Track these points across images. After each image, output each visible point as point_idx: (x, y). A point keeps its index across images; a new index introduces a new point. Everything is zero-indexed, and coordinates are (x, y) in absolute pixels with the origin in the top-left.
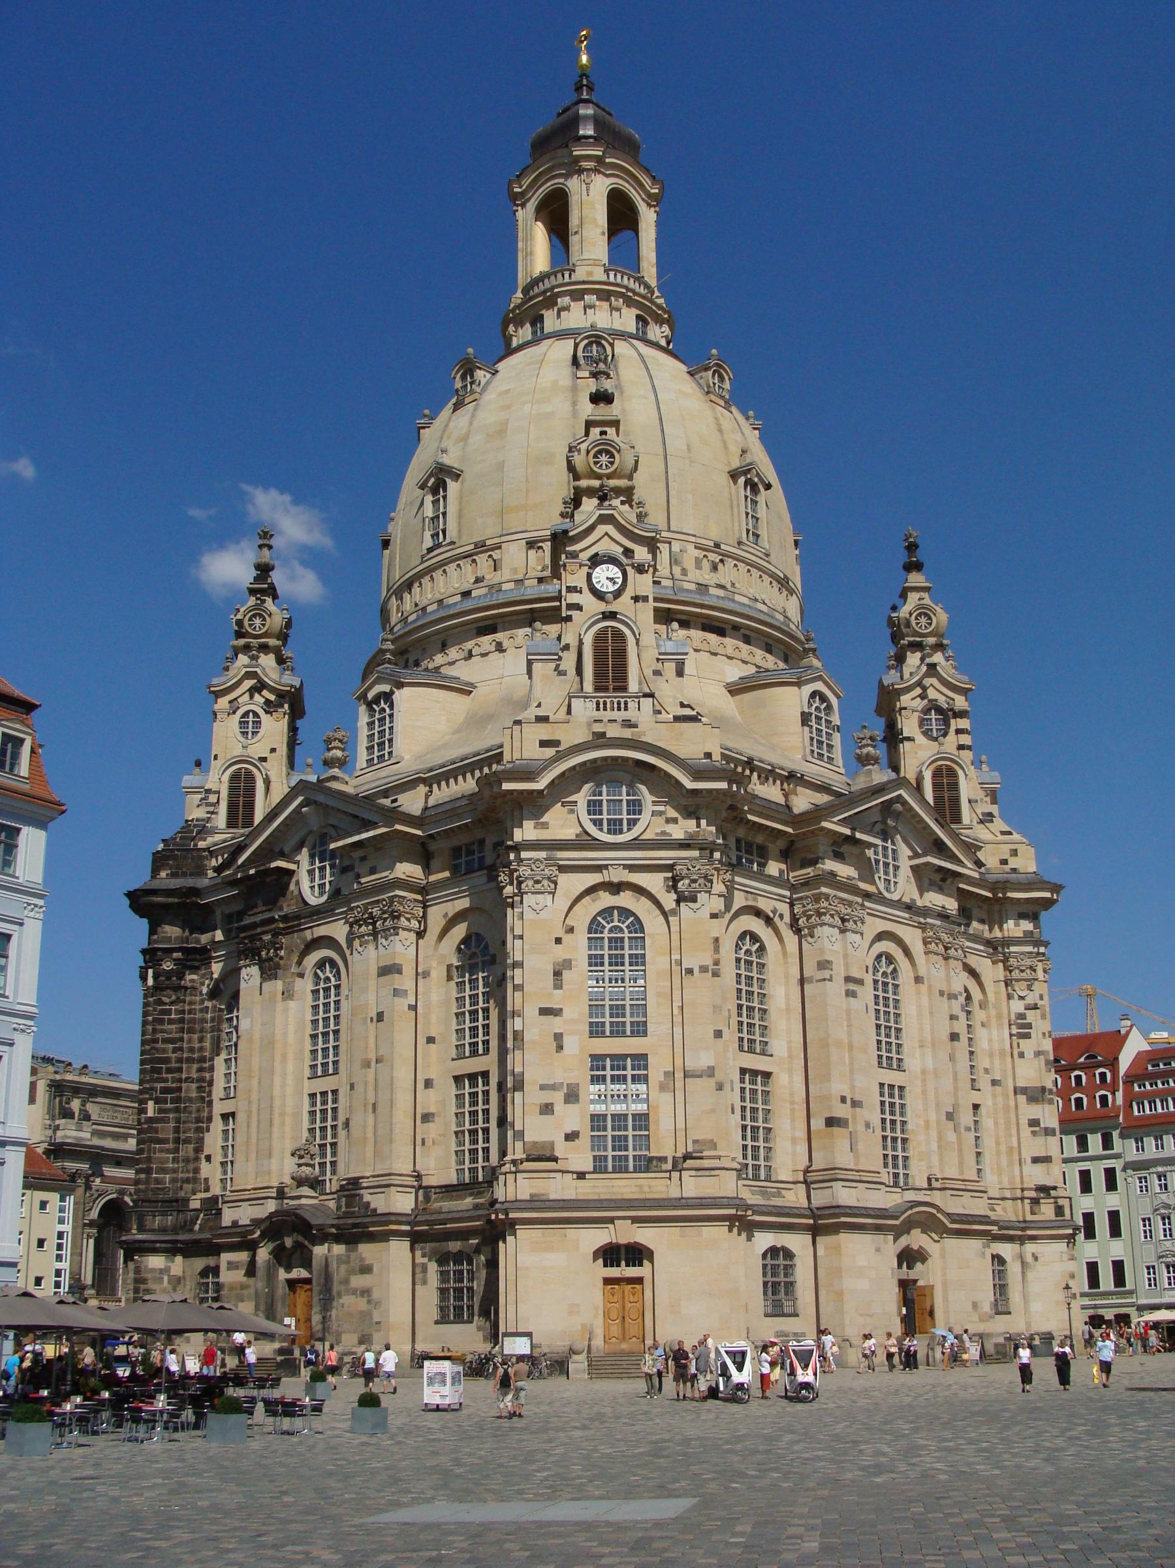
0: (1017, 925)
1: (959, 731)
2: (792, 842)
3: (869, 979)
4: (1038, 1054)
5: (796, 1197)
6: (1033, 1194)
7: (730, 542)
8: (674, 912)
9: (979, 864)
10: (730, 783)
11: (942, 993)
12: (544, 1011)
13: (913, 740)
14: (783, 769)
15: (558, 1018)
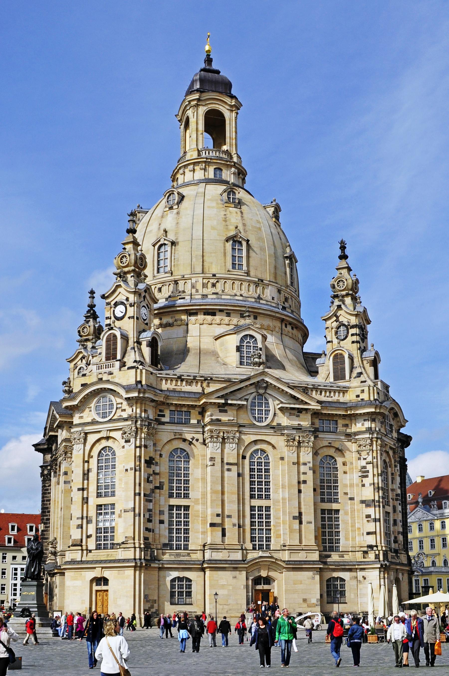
0: (363, 425)
1: (352, 335)
2: (203, 408)
3: (247, 461)
4: (370, 485)
5: (198, 556)
6: (365, 549)
7: (223, 272)
8: (123, 447)
9: (319, 402)
10: (139, 393)
11: (294, 463)
12: (79, 489)
13: (332, 342)
14: (201, 377)
15: (85, 492)
